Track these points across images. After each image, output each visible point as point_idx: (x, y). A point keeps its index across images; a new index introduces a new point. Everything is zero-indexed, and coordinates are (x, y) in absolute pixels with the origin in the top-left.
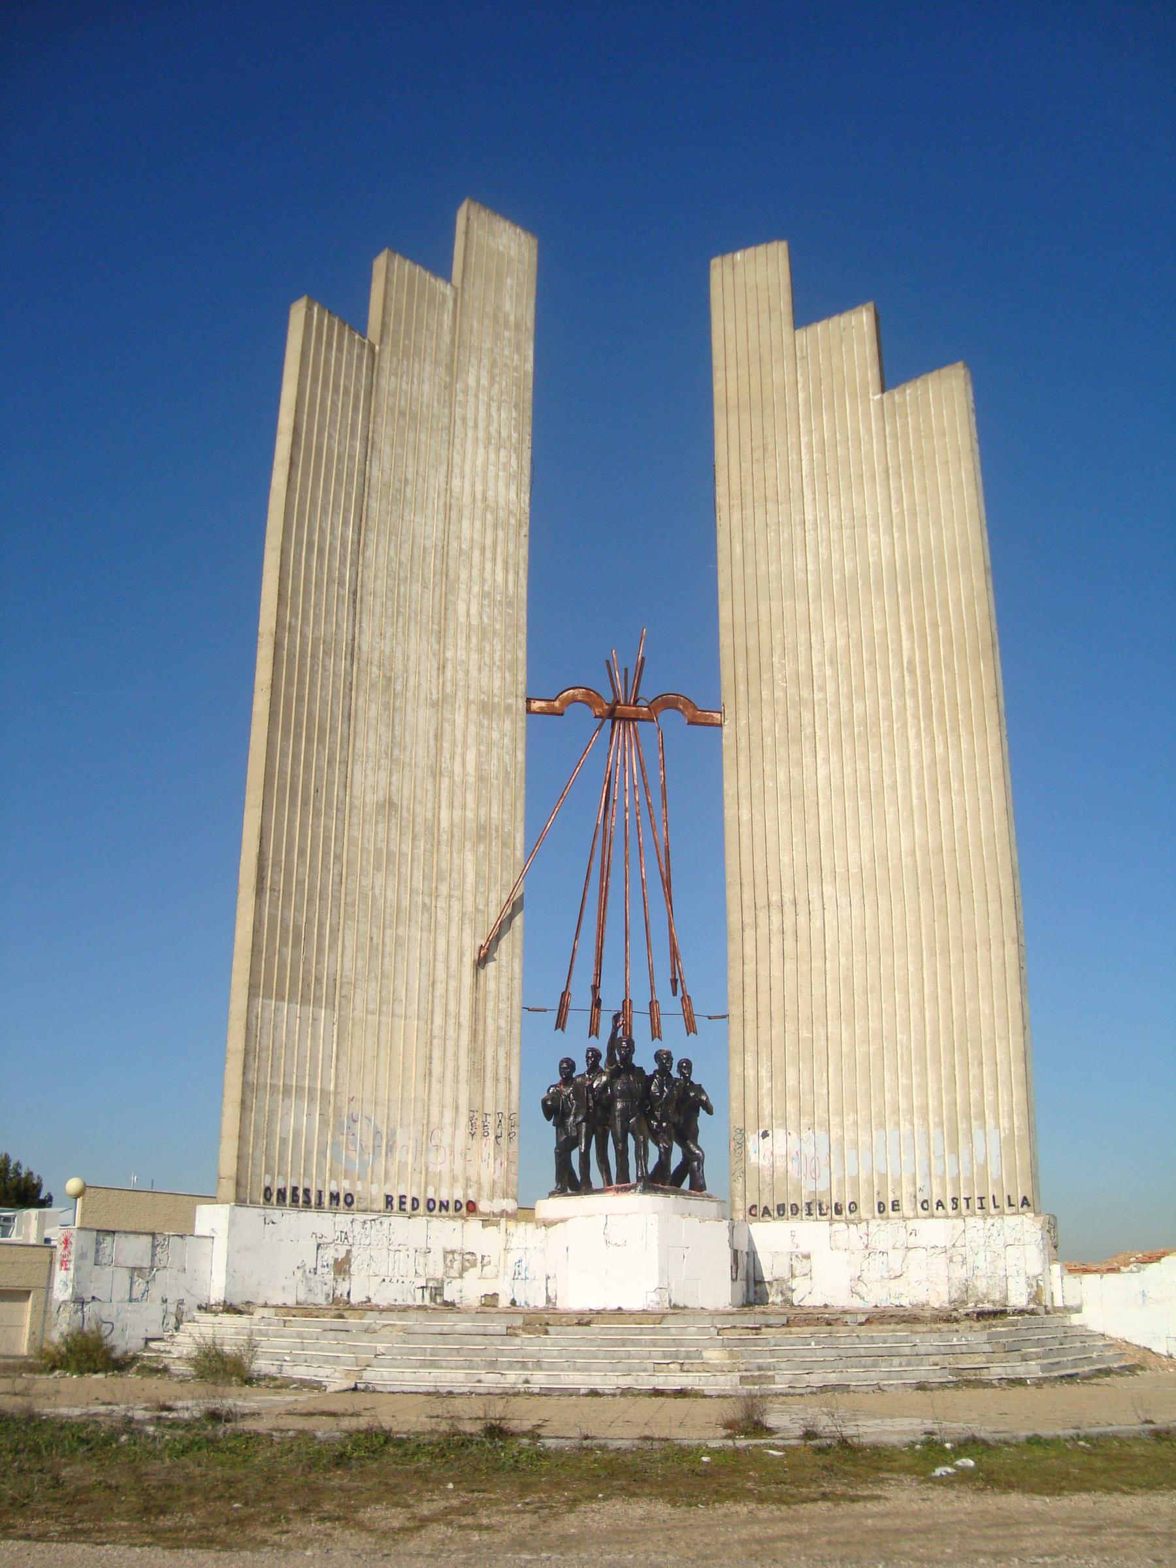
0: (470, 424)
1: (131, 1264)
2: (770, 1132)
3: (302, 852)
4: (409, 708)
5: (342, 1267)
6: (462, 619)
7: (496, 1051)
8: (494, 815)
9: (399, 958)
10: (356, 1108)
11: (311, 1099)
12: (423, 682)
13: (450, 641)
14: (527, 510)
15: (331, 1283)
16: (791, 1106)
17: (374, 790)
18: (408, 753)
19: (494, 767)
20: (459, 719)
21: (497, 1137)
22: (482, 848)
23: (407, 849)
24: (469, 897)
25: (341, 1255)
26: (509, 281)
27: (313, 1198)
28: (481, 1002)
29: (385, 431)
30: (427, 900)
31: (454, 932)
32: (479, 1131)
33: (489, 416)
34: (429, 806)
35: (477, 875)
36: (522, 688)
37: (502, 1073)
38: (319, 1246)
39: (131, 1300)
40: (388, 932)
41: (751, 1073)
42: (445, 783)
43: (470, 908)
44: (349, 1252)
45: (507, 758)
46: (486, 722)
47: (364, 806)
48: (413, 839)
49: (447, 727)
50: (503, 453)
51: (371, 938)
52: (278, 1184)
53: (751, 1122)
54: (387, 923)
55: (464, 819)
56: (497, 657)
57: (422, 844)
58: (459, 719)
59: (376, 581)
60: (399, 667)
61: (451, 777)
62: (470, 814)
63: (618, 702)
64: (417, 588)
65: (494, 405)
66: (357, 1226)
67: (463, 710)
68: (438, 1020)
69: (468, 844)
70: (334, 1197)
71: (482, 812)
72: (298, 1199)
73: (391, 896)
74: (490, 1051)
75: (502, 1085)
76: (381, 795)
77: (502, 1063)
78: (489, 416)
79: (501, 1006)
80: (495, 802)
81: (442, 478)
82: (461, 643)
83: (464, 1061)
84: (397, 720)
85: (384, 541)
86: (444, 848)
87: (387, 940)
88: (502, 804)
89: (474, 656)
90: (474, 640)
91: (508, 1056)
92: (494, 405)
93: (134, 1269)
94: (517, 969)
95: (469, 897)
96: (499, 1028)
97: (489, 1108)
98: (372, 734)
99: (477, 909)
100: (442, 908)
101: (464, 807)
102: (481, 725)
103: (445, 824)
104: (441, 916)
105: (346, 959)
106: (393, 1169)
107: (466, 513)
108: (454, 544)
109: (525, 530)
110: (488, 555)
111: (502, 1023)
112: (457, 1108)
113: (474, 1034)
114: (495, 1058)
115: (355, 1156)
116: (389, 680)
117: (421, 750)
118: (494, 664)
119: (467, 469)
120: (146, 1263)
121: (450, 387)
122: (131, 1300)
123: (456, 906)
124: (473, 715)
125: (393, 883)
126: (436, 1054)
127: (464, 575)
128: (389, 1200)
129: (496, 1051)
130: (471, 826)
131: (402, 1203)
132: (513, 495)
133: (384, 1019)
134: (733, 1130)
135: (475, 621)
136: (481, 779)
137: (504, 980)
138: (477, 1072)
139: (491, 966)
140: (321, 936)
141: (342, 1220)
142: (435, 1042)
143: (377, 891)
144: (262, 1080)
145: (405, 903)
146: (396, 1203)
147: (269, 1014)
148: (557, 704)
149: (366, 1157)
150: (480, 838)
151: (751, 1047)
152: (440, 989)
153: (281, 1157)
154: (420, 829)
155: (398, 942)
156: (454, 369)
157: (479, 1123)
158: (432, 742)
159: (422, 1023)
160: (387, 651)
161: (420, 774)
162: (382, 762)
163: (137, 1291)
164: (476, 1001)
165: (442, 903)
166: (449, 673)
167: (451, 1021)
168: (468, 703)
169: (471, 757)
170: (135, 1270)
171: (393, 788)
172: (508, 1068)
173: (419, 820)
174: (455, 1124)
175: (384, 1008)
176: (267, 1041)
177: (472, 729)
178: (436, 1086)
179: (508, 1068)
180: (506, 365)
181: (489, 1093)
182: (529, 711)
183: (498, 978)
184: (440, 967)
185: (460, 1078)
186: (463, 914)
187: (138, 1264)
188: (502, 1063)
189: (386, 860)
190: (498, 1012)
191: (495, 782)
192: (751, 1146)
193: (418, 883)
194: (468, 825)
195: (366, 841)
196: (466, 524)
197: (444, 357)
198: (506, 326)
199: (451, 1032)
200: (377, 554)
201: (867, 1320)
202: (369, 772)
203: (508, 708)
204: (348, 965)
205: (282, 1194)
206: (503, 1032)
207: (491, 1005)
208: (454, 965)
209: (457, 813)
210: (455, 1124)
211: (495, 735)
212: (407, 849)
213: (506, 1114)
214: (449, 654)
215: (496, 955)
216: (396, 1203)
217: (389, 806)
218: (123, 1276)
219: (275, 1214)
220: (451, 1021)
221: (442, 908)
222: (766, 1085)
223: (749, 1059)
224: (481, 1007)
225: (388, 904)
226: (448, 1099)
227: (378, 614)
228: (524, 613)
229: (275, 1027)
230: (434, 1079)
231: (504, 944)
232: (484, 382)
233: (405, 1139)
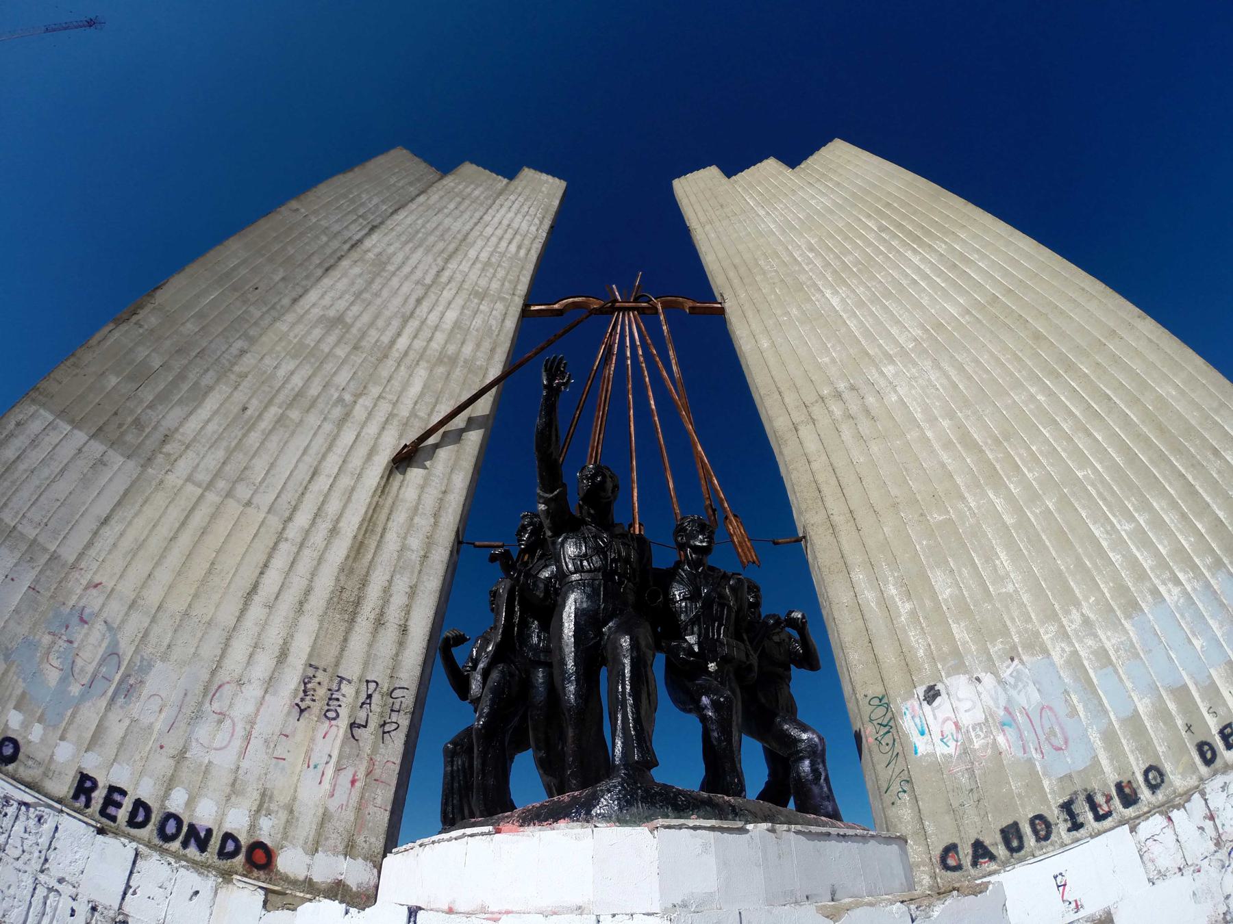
2: (939, 687)
7: (390, 582)
9: (275, 438)
16: (960, 632)
19: (478, 322)
21: (353, 725)
22: (441, 370)
23: (341, 352)
28: (386, 511)
30: (348, 397)
31: (372, 429)
32: (317, 708)
35: (425, 386)
37: (394, 615)
40: (274, 411)
41: (869, 596)
42: (413, 324)
43: (404, 411)
47: (307, 312)
48: (356, 348)
51: (245, 409)
53: (895, 679)
54: (277, 401)
55: (425, 349)
58: (447, 294)
61: (423, 322)
63: (616, 301)
67: (453, 292)
68: (303, 519)
69: (423, 364)
74: (378, 580)
75: (389, 635)
76: (332, 313)
77: (398, 599)
79: (417, 519)
83: (325, 582)
86: (390, 363)
88: (478, 345)
91: (413, 592)
94: (460, 482)
96: (403, 548)
97: (351, 668)
99: (413, 413)
100: (366, 408)
101: (431, 339)
104: (359, 412)
105: (202, 420)
111: (415, 542)
112: (283, 656)
113: (358, 548)
114: (387, 591)
117: (397, 302)
118: (494, 275)
123: (384, 408)
124: (464, 295)
125: (306, 371)
126: (280, 562)
129: (390, 582)
133: (212, 498)
134: (863, 703)
136: (457, 324)
138: (346, 604)
139: (415, 474)
142: (284, 547)
145: (314, 390)
148: (556, 306)
151: (855, 558)
152: (322, 483)
155: (280, 420)
157: (322, 692)
158: (412, 301)
159: (275, 522)
161: (387, 313)
162: (347, 296)
164: (375, 508)
167: (323, 527)
168: (460, 289)
169: (451, 316)
172: (408, 609)
175: (221, 484)
177: (459, 301)
178: (256, 611)
179: (408, 609)
181: (358, 642)
182: (525, 312)
183: (422, 488)
184: (332, 463)
185: (307, 607)
186: (391, 416)
188: (398, 599)
190: (410, 525)
191: (475, 333)
192: (908, 724)
193: (343, 378)
194: (428, 352)
195: (292, 334)
199: (319, 537)
203: (503, 299)
206: (414, 557)
207: (400, 517)
209: (419, 344)
213: (385, 687)
215: (428, 463)
220: (323, 527)
221: (366, 408)
222: (904, 608)
223: (859, 576)
224: (383, 517)
225: (289, 386)
226: (274, 636)
230: (258, 599)
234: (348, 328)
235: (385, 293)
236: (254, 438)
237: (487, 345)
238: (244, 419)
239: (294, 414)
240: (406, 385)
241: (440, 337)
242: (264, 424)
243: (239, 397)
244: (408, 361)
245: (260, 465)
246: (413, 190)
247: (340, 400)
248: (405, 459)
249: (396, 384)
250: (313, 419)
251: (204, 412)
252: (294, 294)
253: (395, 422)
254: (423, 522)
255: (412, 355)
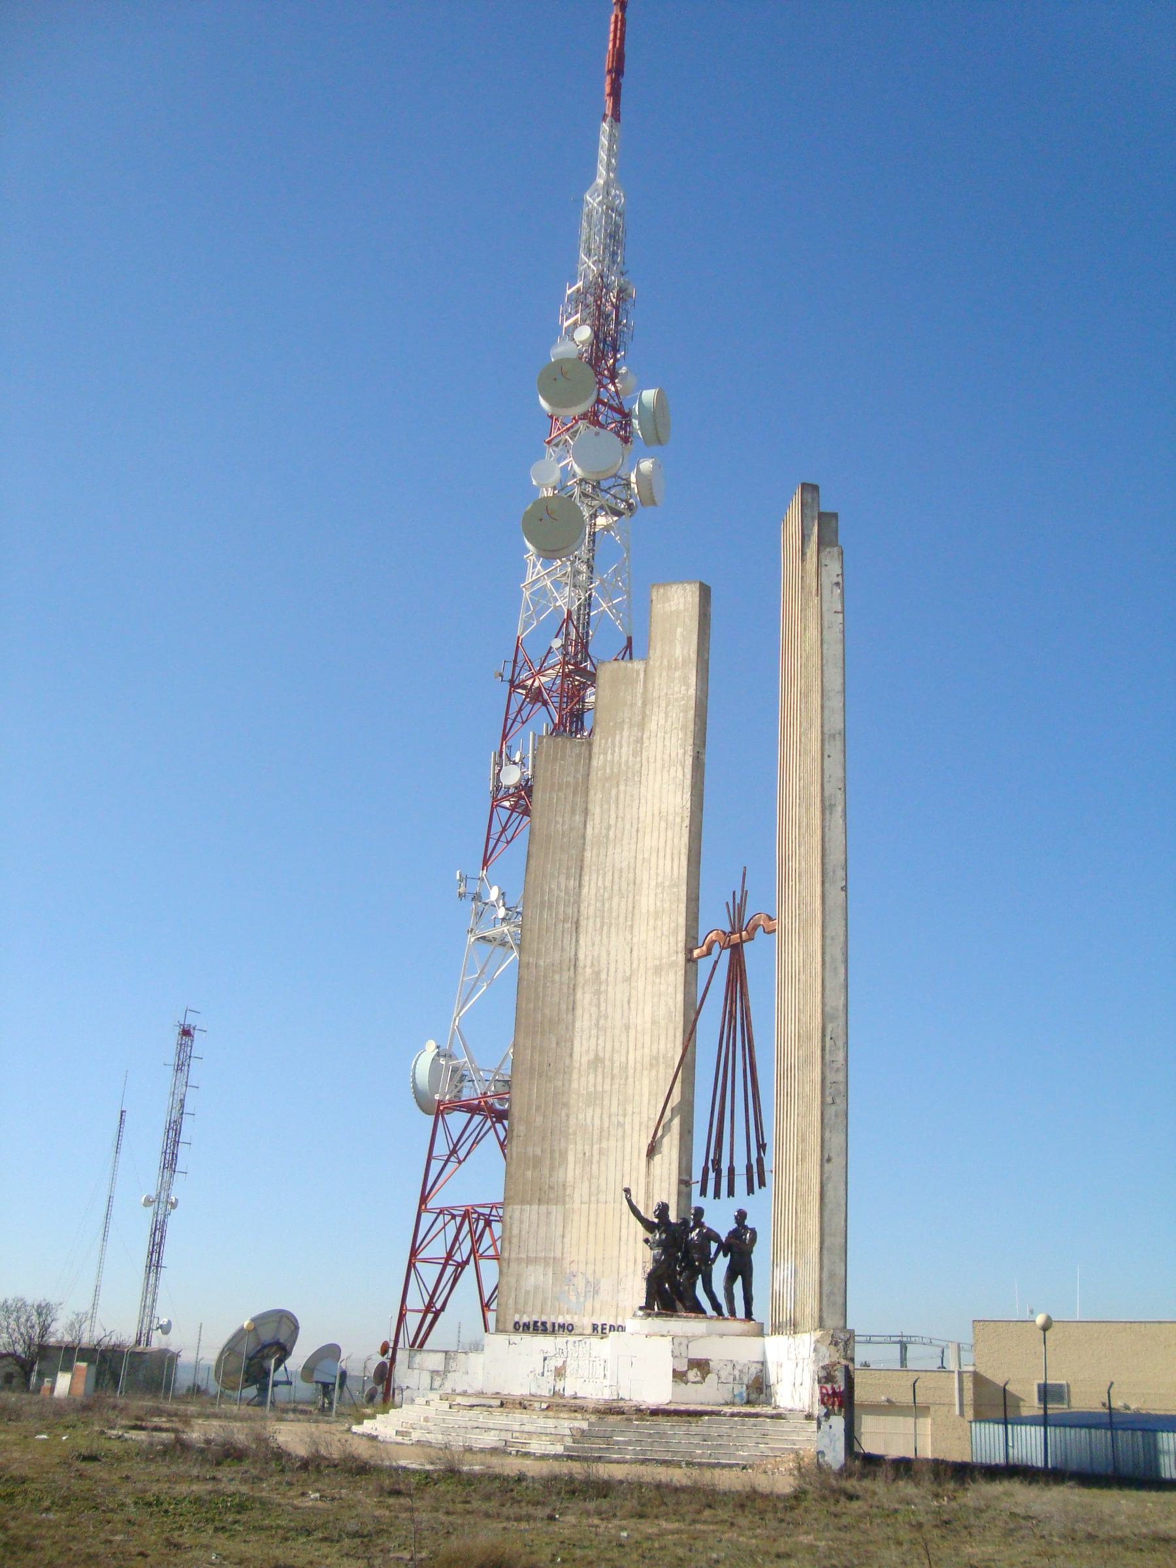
0: (652, 760)
1: (431, 1368)
3: (538, 1108)
4: (610, 989)
5: (560, 1373)
6: (644, 911)
8: (662, 1047)
9: (602, 1163)
10: (574, 1267)
11: (547, 1264)
12: (620, 965)
13: (636, 930)
14: (689, 805)
15: (552, 1382)
17: (588, 1052)
18: (609, 1020)
20: (641, 984)
22: (654, 1073)
23: (607, 1087)
24: (645, 1109)
25: (560, 1364)
26: (679, 630)
27: (549, 1326)
29: (596, 796)
30: (621, 1119)
31: (636, 1137)
33: (664, 746)
34: (624, 1052)
36: (681, 945)
38: (545, 1359)
39: (431, 1389)
40: (596, 1147)
42: (632, 1032)
44: (565, 1362)
45: (671, 1003)
46: (657, 980)
48: (612, 1079)
49: (634, 993)
50: (673, 769)
52: (526, 1319)
56: (665, 928)
57: (617, 1081)
58: (641, 984)
59: (589, 909)
60: (604, 961)
62: (647, 1051)
64: (616, 900)
65: (667, 736)
66: (570, 1345)
69: (646, 1073)
70: (562, 1326)
71: (655, 1047)
72: (539, 1328)
73: (597, 1122)
76: (592, 1056)
78: (664, 746)
80: (663, 1038)
81: (635, 810)
82: (643, 928)
84: (602, 1000)
85: (594, 877)
86: (630, 1080)
87: (596, 1152)
89: (651, 933)
90: (651, 922)
92: (667, 736)
93: (433, 1372)
95: (645, 1109)
98: (586, 1016)
99: (649, 1118)
102: (654, 983)
103: (631, 1063)
105: (571, 1171)
106: (597, 1306)
107: (648, 830)
108: (640, 857)
109: (687, 822)
110: (661, 854)
115: (573, 1298)
116: (598, 973)
119: (649, 797)
120: (441, 1368)
121: (640, 741)
122: (431, 1389)
123: (636, 1118)
127: (645, 878)
128: (595, 1327)
130: (647, 1059)
131: (603, 1329)
132: (679, 800)
133: (593, 1206)
135: (652, 909)
136: (653, 1022)
137: (666, 1165)
139: (657, 1158)
140: (552, 1158)
141: (560, 1340)
143: (589, 1121)
144: (513, 1255)
145: (606, 1125)
146: (599, 1329)
147: (517, 1214)
149: (582, 1299)
150: (651, 1065)
153: (526, 1303)
154: (616, 1071)
155: (600, 1152)
156: (642, 726)
160: (596, 954)
163: (436, 1384)
164: (648, 1184)
165: (628, 1119)
166: (635, 953)
170: (434, 1373)
171: (600, 1048)
173: (617, 1064)
174: (634, 1272)
175: (593, 1198)
176: (515, 1231)
177: (649, 988)
180: (676, 700)
186: (641, 1124)
187: (436, 1368)
189: (594, 1099)
196: (648, 837)
197: (638, 718)
198: (676, 669)
200: (589, 890)
201: (548, 1408)
202: (584, 1042)
204: (570, 1174)
205: (526, 1327)
208: (635, 1162)
209: (639, 1053)
210: (634, 1272)
211: (663, 988)
212: (607, 1087)
214: (635, 940)
216: (599, 1329)
217: (597, 1061)
218: (426, 1379)
219: (516, 1338)
227: (590, 930)
228: (684, 887)
229: (521, 1222)
231: (666, 1140)
232: (662, 722)
233: (606, 1285)
234: (602, 1061)
235: (610, 1010)
236: (595, 1167)
237: (671, 1032)
238: (587, 1161)
239: (604, 1145)
240: (641, 1095)
241: (647, 1038)
242: (596, 1158)
243: (580, 1147)
244: (638, 1075)
245: (602, 1182)
246: (578, 818)
247: (619, 1123)
248: (652, 1151)
249: (637, 1098)
250: (612, 1143)
251: (571, 1166)
252: (568, 1052)
253: (643, 1128)
254: (665, 1185)
255: (639, 1066)
